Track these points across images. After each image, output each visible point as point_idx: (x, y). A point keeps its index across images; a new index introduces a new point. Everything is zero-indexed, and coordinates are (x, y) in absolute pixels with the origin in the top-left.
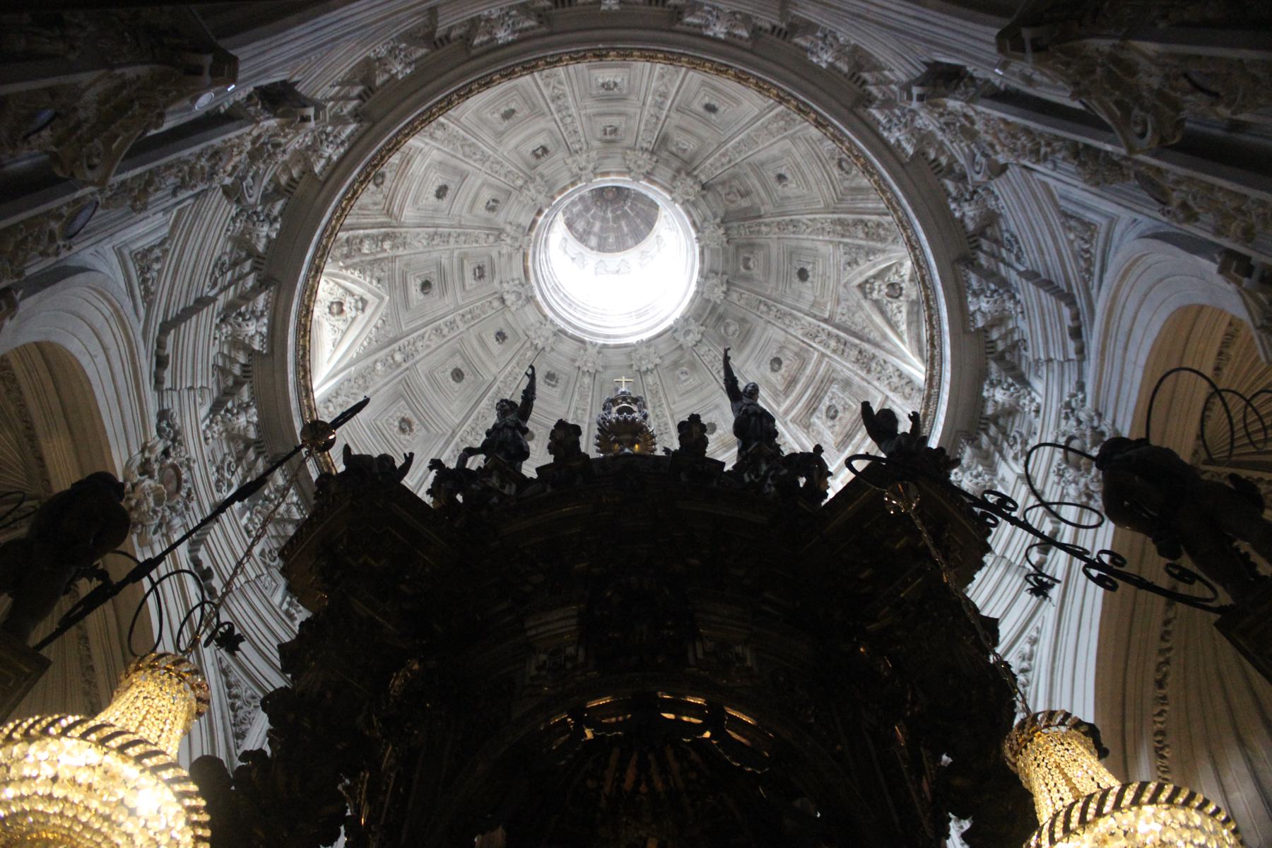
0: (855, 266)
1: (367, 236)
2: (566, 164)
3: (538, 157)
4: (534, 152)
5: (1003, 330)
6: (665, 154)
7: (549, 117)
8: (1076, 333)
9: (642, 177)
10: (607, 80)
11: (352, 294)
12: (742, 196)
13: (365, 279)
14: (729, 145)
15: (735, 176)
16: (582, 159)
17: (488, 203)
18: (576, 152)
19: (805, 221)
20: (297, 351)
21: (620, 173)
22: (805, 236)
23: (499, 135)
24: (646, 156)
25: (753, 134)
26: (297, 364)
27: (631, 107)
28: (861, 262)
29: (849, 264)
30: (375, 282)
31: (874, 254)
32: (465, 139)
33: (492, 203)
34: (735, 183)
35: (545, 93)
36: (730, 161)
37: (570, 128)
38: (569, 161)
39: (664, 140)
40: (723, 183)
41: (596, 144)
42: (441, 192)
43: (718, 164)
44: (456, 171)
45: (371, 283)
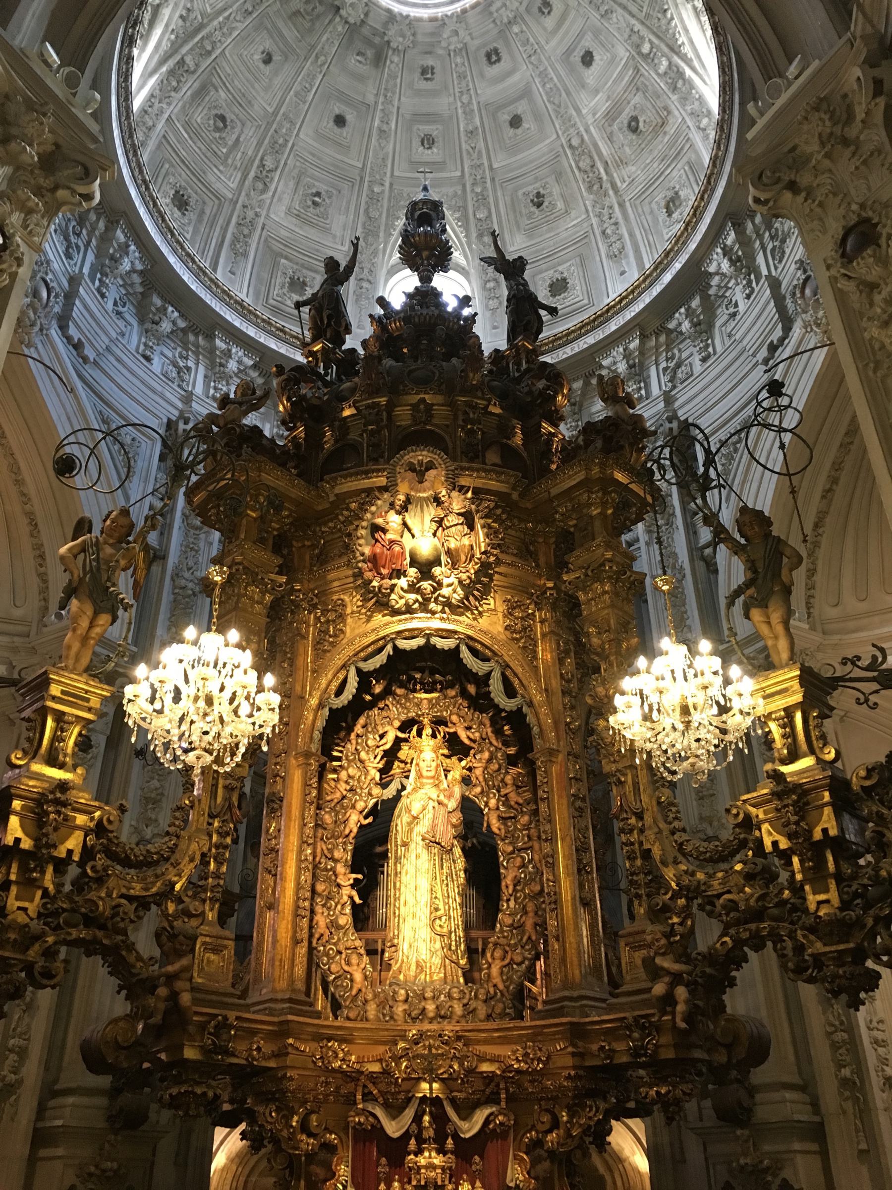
0: (184, 13)
1: (658, 74)
2: (470, 34)
3: (496, 51)
4: (499, 60)
5: (97, 233)
6: (377, 40)
7: (482, 99)
8: (78, 346)
9: (398, 19)
10: (429, 152)
11: (695, 8)
12: (299, 12)
13: (676, 26)
14: (320, 77)
15: (310, 30)
16: (455, 44)
17: (549, 13)
18: (461, 50)
19: (238, 24)
20: (710, 197)
21: (419, 20)
22: (235, 7)
23: (526, 93)
24: (394, 45)
25: (302, 105)
26: (713, 191)
27: (409, 103)
28: (180, 22)
29: (189, 10)
30: (669, 16)
31: (173, 43)
32: (556, 111)
33: (546, 11)
34: (307, 25)
35: (481, 145)
36: (317, 57)
37: (464, 84)
38: (467, 39)
39: (379, 60)
40: (318, 16)
41: (440, 52)
42: (588, 59)
43: (326, 47)
44: (572, 70)
45: (672, 19)
